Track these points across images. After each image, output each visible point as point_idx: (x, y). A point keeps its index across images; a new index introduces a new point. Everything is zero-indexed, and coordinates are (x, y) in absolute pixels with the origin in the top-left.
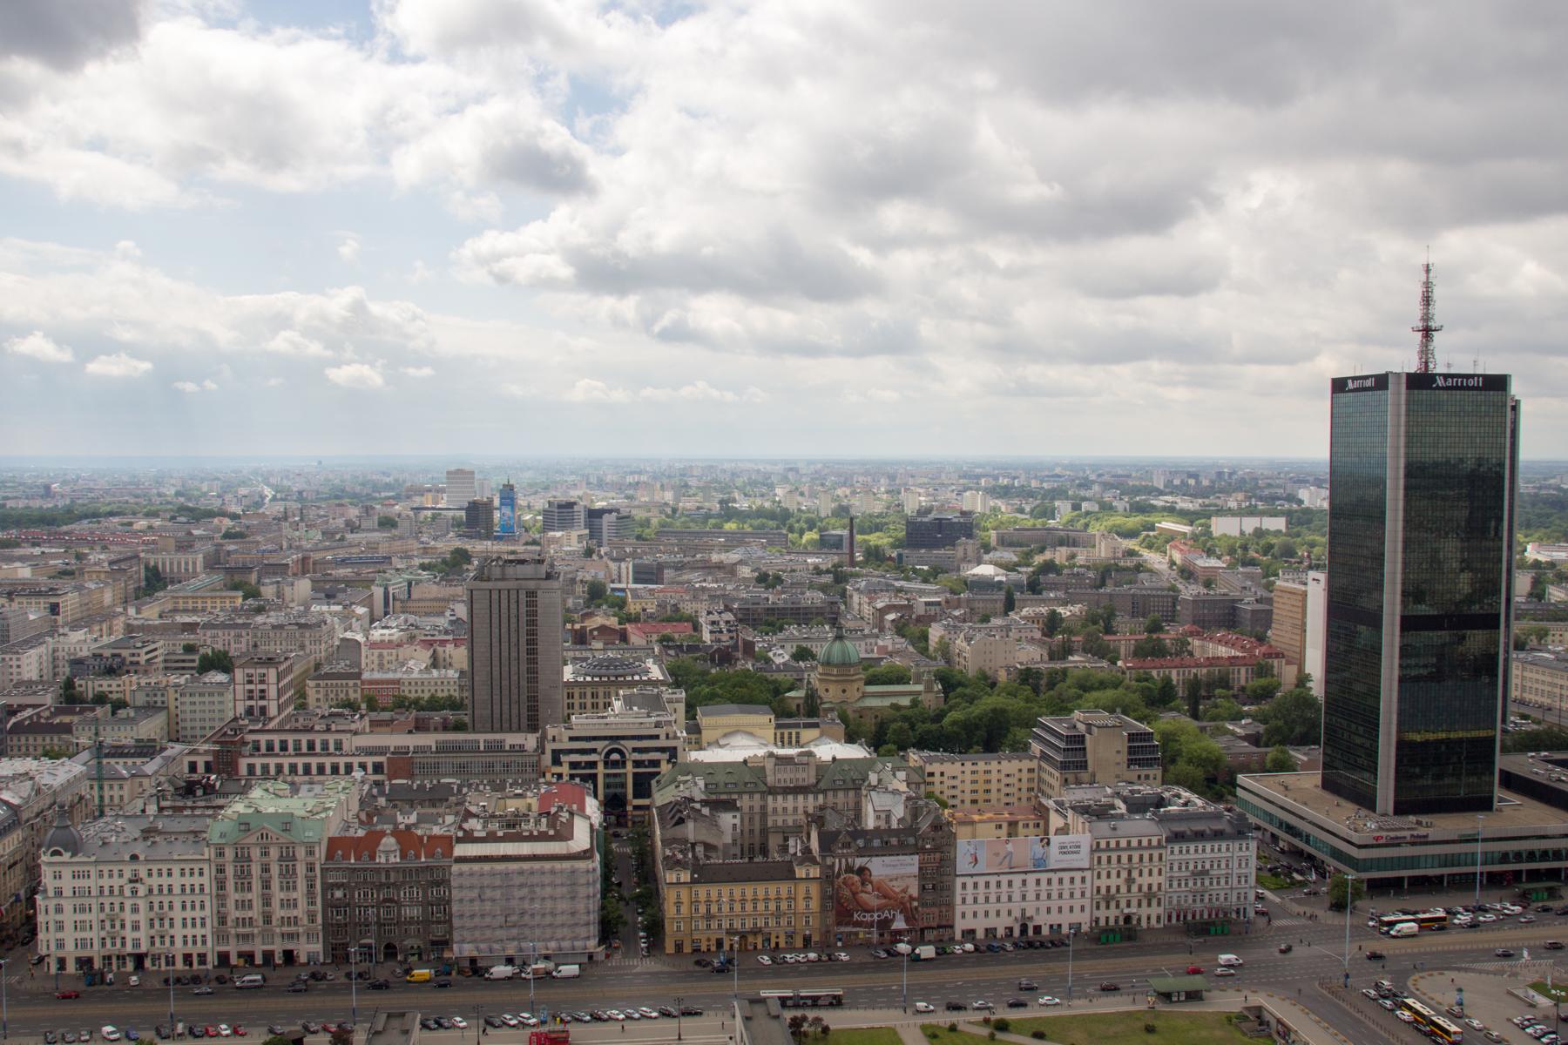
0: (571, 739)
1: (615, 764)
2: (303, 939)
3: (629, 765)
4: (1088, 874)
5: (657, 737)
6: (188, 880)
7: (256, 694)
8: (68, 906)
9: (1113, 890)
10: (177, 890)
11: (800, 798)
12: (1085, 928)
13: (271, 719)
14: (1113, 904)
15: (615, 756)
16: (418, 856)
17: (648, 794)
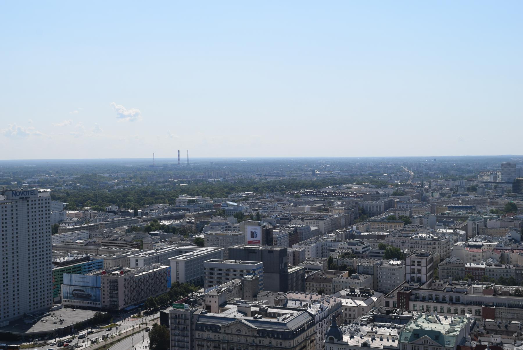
7: (416, 271)
13: (423, 284)
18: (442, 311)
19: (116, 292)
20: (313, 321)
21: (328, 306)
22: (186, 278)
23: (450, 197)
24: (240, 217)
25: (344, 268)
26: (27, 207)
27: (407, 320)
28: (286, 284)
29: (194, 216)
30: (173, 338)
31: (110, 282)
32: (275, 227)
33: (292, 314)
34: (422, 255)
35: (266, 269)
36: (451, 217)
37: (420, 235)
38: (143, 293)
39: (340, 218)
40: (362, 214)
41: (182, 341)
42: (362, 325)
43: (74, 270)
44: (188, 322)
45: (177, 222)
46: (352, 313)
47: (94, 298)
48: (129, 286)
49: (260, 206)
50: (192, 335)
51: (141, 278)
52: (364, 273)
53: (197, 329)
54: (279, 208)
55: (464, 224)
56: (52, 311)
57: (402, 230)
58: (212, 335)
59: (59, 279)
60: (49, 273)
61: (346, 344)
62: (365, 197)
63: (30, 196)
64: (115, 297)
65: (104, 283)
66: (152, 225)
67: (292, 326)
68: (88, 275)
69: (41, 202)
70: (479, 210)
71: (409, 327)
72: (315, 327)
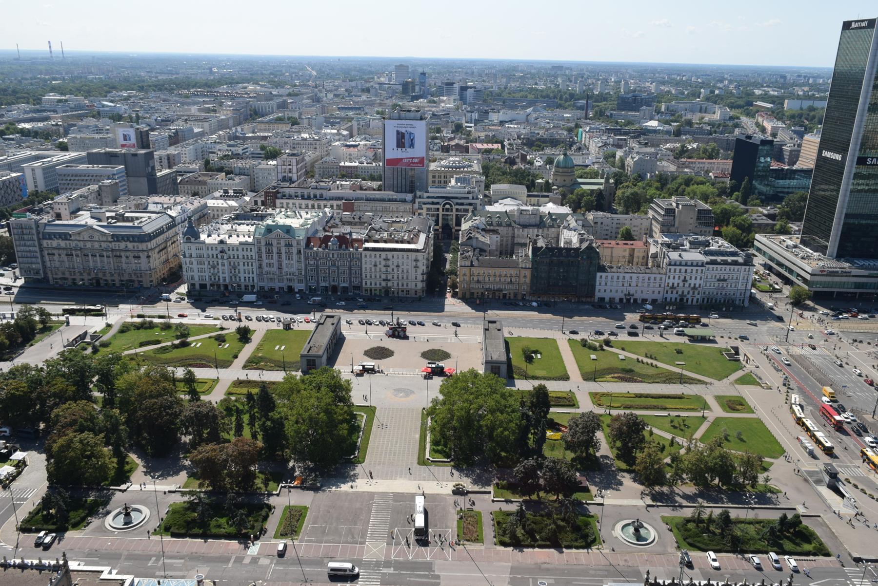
0: (428, 197)
1: (447, 210)
2: (296, 281)
3: (454, 210)
4: (664, 276)
5: (468, 198)
6: (245, 253)
8: (195, 263)
9: (676, 285)
10: (241, 257)
11: (531, 230)
12: (659, 301)
13: (293, 182)
14: (675, 292)
15: (447, 206)
16: (347, 247)
17: (460, 225)
18: (307, 207)
20: (173, 223)
21: (190, 208)
22: (46, 186)
23: (343, 98)
24: (117, 117)
25: (221, 170)
27: (262, 218)
28: (154, 187)
29: (62, 117)
30: (19, 248)
32: (153, 130)
33: (150, 218)
34: (294, 155)
35: (128, 173)
36: (338, 118)
37: (302, 135)
39: (228, 119)
40: (253, 115)
41: (30, 251)
42: (222, 224)
44: (34, 231)
45: (40, 125)
46: (216, 213)
49: (141, 107)
50: (40, 245)
52: (240, 174)
53: (44, 238)
54: (163, 109)
55: (350, 124)
57: (288, 131)
58: (63, 244)
61: (204, 242)
62: (258, 97)
66: (8, 129)
67: (148, 229)
70: (367, 111)
71: (265, 223)
72: (176, 229)
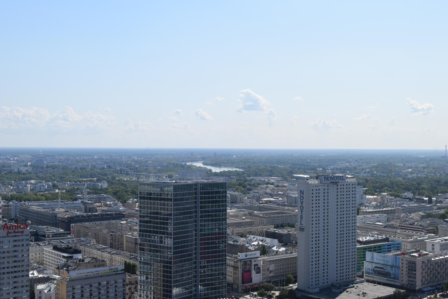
19: (414, 273)
26: (336, 190)
31: (409, 263)
38: (439, 276)
43: (375, 249)
47: (393, 276)
48: (427, 269)
51: (438, 262)
56: (356, 284)
59: (362, 256)
60: (353, 250)
63: (339, 181)
64: (412, 277)
65: (402, 264)
68: (388, 254)
69: (348, 187)
